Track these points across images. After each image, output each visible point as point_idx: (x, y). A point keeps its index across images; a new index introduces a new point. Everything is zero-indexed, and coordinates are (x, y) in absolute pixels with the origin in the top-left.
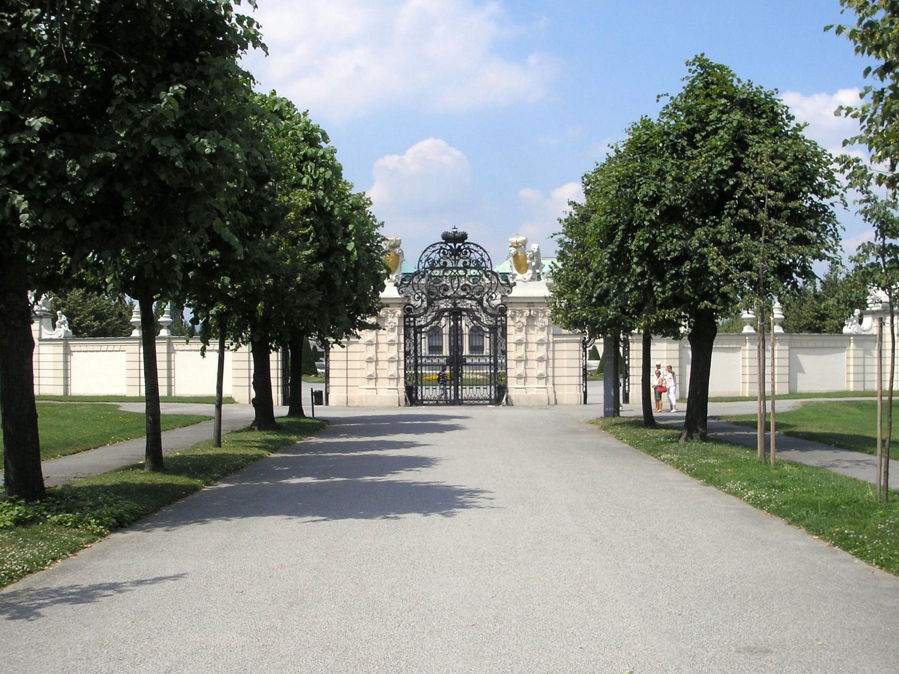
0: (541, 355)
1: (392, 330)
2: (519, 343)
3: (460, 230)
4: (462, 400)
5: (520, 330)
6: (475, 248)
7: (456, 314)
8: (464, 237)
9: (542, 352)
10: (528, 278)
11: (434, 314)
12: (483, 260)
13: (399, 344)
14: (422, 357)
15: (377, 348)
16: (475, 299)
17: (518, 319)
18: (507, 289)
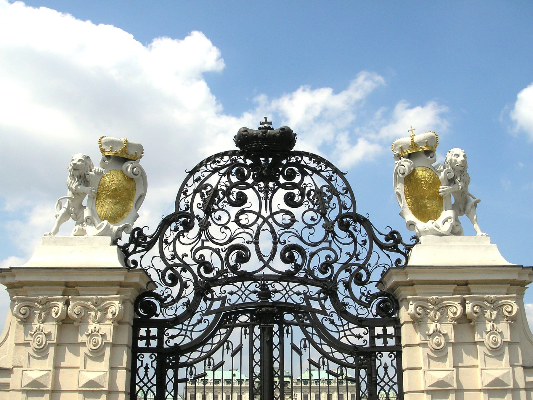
1: (97, 354)
3: (276, 127)
5: (439, 354)
7: (267, 315)
8: (287, 137)
10: (446, 228)
11: (211, 318)
16: (316, 282)
17: (432, 327)
18: (395, 256)
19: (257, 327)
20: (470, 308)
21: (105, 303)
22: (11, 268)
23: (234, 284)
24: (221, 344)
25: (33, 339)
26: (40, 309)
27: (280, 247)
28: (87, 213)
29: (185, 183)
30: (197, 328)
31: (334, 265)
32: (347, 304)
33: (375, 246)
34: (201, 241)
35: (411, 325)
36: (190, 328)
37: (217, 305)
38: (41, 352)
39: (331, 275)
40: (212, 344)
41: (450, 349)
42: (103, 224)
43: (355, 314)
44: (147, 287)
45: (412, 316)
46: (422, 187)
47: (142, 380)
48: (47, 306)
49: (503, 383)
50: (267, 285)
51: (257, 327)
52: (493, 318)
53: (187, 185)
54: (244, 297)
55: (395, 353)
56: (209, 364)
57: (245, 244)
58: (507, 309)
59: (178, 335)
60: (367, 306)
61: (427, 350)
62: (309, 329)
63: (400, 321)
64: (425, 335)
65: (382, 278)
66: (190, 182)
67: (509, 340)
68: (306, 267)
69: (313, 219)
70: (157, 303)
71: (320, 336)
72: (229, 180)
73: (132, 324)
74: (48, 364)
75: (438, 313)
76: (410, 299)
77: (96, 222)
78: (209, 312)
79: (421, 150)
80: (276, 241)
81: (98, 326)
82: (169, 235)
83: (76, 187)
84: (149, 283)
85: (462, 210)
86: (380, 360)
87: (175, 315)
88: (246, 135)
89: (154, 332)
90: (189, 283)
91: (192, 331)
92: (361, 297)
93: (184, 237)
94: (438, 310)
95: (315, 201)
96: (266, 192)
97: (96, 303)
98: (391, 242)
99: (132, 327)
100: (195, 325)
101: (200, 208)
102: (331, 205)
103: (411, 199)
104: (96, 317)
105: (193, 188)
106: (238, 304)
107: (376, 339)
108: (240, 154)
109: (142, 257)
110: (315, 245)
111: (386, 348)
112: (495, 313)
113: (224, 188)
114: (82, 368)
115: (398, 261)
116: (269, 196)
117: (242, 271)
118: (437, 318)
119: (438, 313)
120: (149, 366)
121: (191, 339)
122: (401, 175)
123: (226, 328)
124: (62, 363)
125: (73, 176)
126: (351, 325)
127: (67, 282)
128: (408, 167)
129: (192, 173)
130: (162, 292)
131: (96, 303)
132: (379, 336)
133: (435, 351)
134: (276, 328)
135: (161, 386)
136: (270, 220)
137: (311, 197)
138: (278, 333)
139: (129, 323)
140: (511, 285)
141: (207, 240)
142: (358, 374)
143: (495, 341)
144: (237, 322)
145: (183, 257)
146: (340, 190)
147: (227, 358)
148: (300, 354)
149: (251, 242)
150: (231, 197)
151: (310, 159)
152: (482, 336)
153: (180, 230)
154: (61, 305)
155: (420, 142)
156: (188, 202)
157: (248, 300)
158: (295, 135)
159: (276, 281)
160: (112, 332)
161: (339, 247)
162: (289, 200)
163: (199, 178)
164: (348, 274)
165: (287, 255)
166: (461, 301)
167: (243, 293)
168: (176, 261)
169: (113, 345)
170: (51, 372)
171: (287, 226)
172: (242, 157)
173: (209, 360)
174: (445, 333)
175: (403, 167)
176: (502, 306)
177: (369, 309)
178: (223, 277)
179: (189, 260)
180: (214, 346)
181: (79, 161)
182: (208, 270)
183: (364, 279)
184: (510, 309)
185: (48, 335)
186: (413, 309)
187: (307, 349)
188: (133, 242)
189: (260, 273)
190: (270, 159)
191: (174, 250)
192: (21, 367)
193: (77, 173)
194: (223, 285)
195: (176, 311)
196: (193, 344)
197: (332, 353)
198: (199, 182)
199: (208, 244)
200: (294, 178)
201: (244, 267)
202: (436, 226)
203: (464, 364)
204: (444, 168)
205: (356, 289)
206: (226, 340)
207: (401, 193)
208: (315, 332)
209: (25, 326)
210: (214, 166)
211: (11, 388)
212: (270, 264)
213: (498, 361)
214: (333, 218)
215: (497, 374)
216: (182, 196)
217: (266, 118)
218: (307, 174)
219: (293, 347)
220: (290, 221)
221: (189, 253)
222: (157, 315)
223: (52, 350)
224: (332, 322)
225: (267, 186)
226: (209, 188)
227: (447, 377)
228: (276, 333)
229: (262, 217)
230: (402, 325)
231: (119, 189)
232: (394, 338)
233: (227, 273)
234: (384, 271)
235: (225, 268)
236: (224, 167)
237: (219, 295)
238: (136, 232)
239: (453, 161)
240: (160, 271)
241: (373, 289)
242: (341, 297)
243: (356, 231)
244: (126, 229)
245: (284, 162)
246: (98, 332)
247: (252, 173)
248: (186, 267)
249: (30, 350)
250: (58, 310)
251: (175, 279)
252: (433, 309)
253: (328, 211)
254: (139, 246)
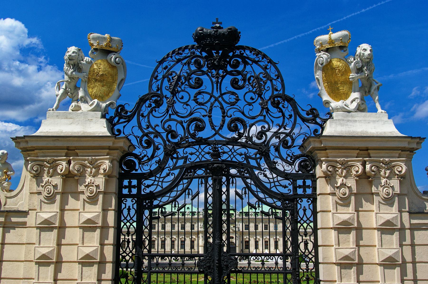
0: (390, 253)
1: (93, 200)
2: (343, 228)
5: (344, 202)
6: (252, 56)
8: (234, 35)
9: (391, 246)
11: (176, 172)
13: (104, 228)
14: (151, 257)
15: (61, 236)
17: (340, 181)
19: (210, 178)
20: (369, 167)
21: (98, 162)
22: (24, 136)
23: (194, 147)
24: (184, 191)
25: (43, 189)
26: (48, 167)
27: (228, 120)
28: (81, 94)
29: (156, 70)
30: (166, 179)
31: (267, 133)
32: (277, 163)
33: (299, 120)
34: (168, 115)
35: (324, 179)
36: (161, 180)
37: (181, 163)
38: (51, 199)
39: (265, 141)
40: (177, 191)
41: (353, 198)
42: (94, 102)
43: (282, 169)
44: (128, 149)
45: (324, 173)
46: (336, 74)
47: (125, 218)
48: (54, 165)
49: (393, 225)
50: (217, 148)
51: (210, 178)
52: (387, 175)
53: (157, 72)
54: (200, 156)
55: (312, 199)
56: (175, 206)
57: (202, 117)
58: (398, 169)
59: (152, 185)
60: (291, 164)
61: (335, 198)
62: (249, 181)
63: (316, 176)
64: (334, 187)
65: (303, 143)
66: (160, 69)
67: (399, 192)
68: (247, 135)
69: (252, 99)
70: (136, 161)
71: (257, 186)
72: (189, 69)
73: (118, 176)
74: (56, 207)
75: (345, 171)
76: (324, 160)
77: (88, 99)
78: (175, 168)
79: (337, 45)
80: (224, 114)
81: (93, 179)
82: (145, 110)
83: (72, 73)
84: (130, 146)
85: (367, 91)
86: (301, 204)
87: (150, 170)
88: (202, 33)
89: (134, 182)
90: (160, 146)
91: (162, 182)
92: (287, 158)
93: (156, 111)
94: (344, 169)
95: (254, 84)
96: (218, 78)
97: (91, 162)
98: (311, 116)
99: (118, 179)
100: (164, 177)
101: (167, 90)
102: (266, 88)
103: (328, 84)
104: (91, 172)
105: (162, 74)
106: (196, 162)
107: (298, 188)
108: (198, 48)
109: (124, 127)
110: (253, 118)
111: (304, 196)
112: (388, 172)
113: (186, 75)
114: (81, 210)
115: (316, 131)
116: (220, 80)
117: (199, 137)
118: (344, 175)
119: (345, 171)
120: (131, 207)
121: (162, 187)
122: (320, 65)
123: (187, 179)
124: (66, 206)
125: (69, 64)
126: (279, 178)
127: (68, 147)
128: (326, 59)
129: (161, 63)
130: (140, 153)
131: (91, 162)
132: (300, 187)
133: (341, 199)
134: (224, 179)
135: (140, 222)
136: (220, 99)
137: (251, 82)
138: (226, 183)
139: (116, 176)
140: (402, 151)
141: (173, 114)
142: (284, 214)
143: (388, 192)
144: (196, 174)
145: (155, 127)
146: (273, 76)
147: (188, 200)
148: (242, 198)
149: (206, 116)
150: (191, 81)
151: (251, 52)
152: (377, 188)
153: (152, 106)
154: (64, 164)
155: (336, 40)
156: (159, 85)
157: (203, 159)
158: (240, 33)
159: (224, 145)
160: (104, 183)
161: (271, 120)
162: (234, 83)
163: (166, 67)
164: (278, 140)
165: (232, 125)
166: (362, 162)
167: (200, 153)
168: (150, 130)
169: (105, 193)
170: (58, 214)
171: (232, 104)
172: (199, 50)
173: (175, 202)
174: (349, 186)
175: (321, 59)
176: (394, 166)
177: (293, 167)
178: (185, 142)
179: (160, 129)
180: (179, 193)
181: (73, 52)
182: (174, 137)
183: (289, 144)
184: (400, 169)
185: (55, 187)
186: (325, 168)
187: (247, 195)
188: (118, 116)
189: (213, 139)
190: (221, 52)
191: (149, 121)
192: (35, 210)
193: (72, 62)
194: (186, 147)
195: (150, 167)
196: (163, 192)
197: (265, 198)
198: (167, 70)
199: (174, 117)
200: (238, 67)
201: (200, 134)
202: (345, 105)
203: (363, 209)
204: (354, 60)
205: (283, 151)
206: (187, 188)
207: (320, 79)
208: (252, 183)
209: (37, 180)
210: (178, 57)
211: (27, 226)
212: (220, 132)
213: (390, 208)
214: (267, 98)
215: (388, 217)
216: (154, 80)
217: (217, 19)
218: (248, 64)
219: (237, 193)
220: (234, 100)
221: (160, 124)
222: (137, 170)
223: (58, 197)
224: (265, 176)
225: (218, 74)
226: (174, 74)
227: (349, 218)
228: (224, 183)
229: (214, 97)
230: (317, 179)
231: (105, 74)
232: (311, 188)
233: (188, 138)
234: (304, 139)
235: (187, 135)
236: (186, 58)
237: (182, 155)
238: (120, 108)
239: (362, 54)
240: (138, 137)
241: (297, 152)
242: (272, 157)
243: (284, 107)
244: (111, 105)
245: (231, 54)
246: (93, 183)
247: (206, 63)
248: (157, 134)
249: (42, 197)
250: (63, 168)
251: (149, 143)
252: (340, 168)
253: (264, 92)
254: (122, 118)
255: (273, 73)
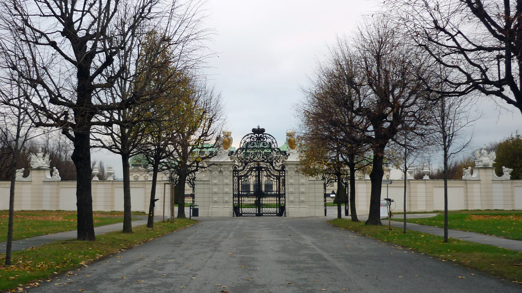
3: (261, 128)
4: (262, 214)
12: (273, 142)
255: (274, 141)
